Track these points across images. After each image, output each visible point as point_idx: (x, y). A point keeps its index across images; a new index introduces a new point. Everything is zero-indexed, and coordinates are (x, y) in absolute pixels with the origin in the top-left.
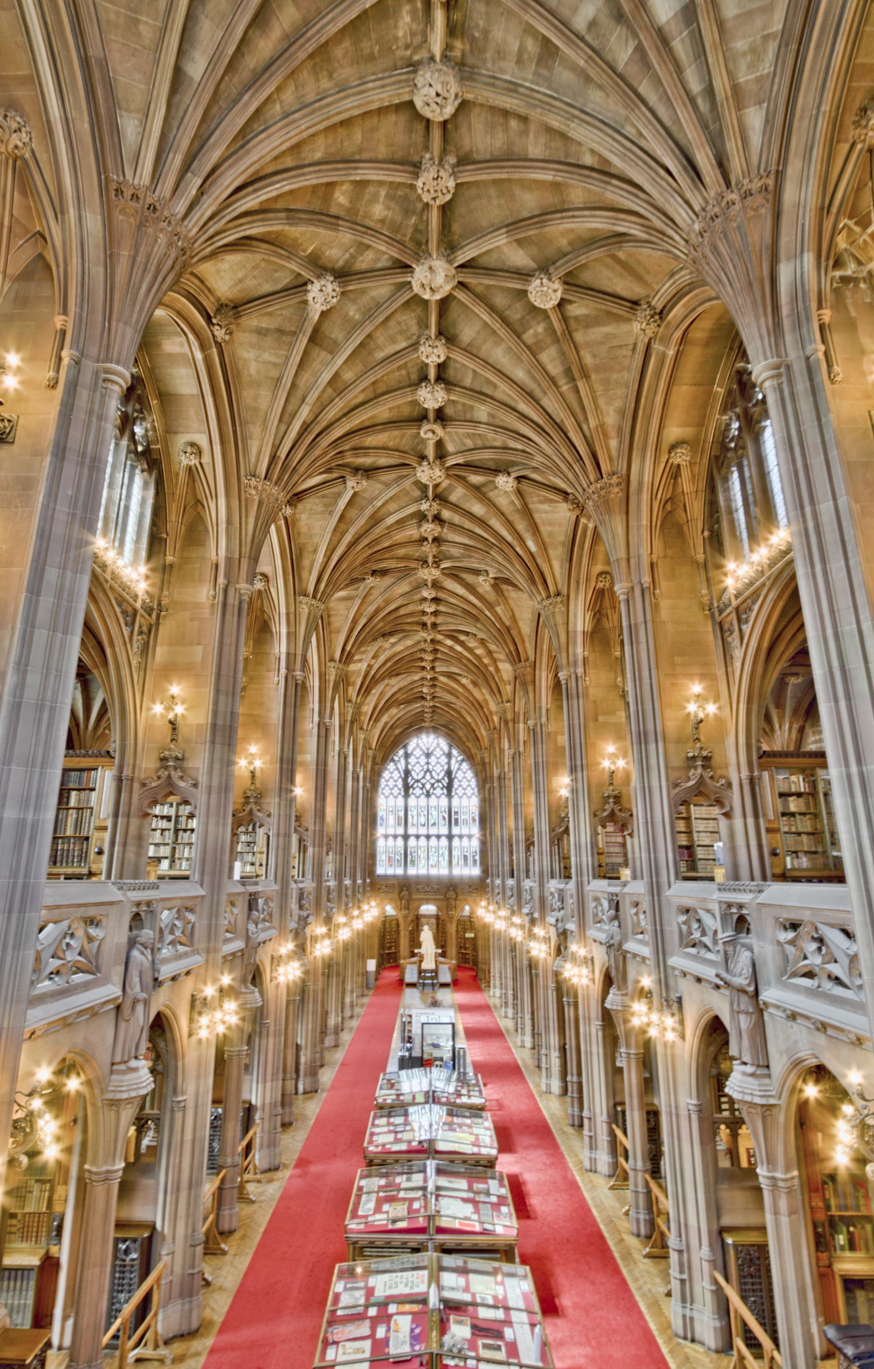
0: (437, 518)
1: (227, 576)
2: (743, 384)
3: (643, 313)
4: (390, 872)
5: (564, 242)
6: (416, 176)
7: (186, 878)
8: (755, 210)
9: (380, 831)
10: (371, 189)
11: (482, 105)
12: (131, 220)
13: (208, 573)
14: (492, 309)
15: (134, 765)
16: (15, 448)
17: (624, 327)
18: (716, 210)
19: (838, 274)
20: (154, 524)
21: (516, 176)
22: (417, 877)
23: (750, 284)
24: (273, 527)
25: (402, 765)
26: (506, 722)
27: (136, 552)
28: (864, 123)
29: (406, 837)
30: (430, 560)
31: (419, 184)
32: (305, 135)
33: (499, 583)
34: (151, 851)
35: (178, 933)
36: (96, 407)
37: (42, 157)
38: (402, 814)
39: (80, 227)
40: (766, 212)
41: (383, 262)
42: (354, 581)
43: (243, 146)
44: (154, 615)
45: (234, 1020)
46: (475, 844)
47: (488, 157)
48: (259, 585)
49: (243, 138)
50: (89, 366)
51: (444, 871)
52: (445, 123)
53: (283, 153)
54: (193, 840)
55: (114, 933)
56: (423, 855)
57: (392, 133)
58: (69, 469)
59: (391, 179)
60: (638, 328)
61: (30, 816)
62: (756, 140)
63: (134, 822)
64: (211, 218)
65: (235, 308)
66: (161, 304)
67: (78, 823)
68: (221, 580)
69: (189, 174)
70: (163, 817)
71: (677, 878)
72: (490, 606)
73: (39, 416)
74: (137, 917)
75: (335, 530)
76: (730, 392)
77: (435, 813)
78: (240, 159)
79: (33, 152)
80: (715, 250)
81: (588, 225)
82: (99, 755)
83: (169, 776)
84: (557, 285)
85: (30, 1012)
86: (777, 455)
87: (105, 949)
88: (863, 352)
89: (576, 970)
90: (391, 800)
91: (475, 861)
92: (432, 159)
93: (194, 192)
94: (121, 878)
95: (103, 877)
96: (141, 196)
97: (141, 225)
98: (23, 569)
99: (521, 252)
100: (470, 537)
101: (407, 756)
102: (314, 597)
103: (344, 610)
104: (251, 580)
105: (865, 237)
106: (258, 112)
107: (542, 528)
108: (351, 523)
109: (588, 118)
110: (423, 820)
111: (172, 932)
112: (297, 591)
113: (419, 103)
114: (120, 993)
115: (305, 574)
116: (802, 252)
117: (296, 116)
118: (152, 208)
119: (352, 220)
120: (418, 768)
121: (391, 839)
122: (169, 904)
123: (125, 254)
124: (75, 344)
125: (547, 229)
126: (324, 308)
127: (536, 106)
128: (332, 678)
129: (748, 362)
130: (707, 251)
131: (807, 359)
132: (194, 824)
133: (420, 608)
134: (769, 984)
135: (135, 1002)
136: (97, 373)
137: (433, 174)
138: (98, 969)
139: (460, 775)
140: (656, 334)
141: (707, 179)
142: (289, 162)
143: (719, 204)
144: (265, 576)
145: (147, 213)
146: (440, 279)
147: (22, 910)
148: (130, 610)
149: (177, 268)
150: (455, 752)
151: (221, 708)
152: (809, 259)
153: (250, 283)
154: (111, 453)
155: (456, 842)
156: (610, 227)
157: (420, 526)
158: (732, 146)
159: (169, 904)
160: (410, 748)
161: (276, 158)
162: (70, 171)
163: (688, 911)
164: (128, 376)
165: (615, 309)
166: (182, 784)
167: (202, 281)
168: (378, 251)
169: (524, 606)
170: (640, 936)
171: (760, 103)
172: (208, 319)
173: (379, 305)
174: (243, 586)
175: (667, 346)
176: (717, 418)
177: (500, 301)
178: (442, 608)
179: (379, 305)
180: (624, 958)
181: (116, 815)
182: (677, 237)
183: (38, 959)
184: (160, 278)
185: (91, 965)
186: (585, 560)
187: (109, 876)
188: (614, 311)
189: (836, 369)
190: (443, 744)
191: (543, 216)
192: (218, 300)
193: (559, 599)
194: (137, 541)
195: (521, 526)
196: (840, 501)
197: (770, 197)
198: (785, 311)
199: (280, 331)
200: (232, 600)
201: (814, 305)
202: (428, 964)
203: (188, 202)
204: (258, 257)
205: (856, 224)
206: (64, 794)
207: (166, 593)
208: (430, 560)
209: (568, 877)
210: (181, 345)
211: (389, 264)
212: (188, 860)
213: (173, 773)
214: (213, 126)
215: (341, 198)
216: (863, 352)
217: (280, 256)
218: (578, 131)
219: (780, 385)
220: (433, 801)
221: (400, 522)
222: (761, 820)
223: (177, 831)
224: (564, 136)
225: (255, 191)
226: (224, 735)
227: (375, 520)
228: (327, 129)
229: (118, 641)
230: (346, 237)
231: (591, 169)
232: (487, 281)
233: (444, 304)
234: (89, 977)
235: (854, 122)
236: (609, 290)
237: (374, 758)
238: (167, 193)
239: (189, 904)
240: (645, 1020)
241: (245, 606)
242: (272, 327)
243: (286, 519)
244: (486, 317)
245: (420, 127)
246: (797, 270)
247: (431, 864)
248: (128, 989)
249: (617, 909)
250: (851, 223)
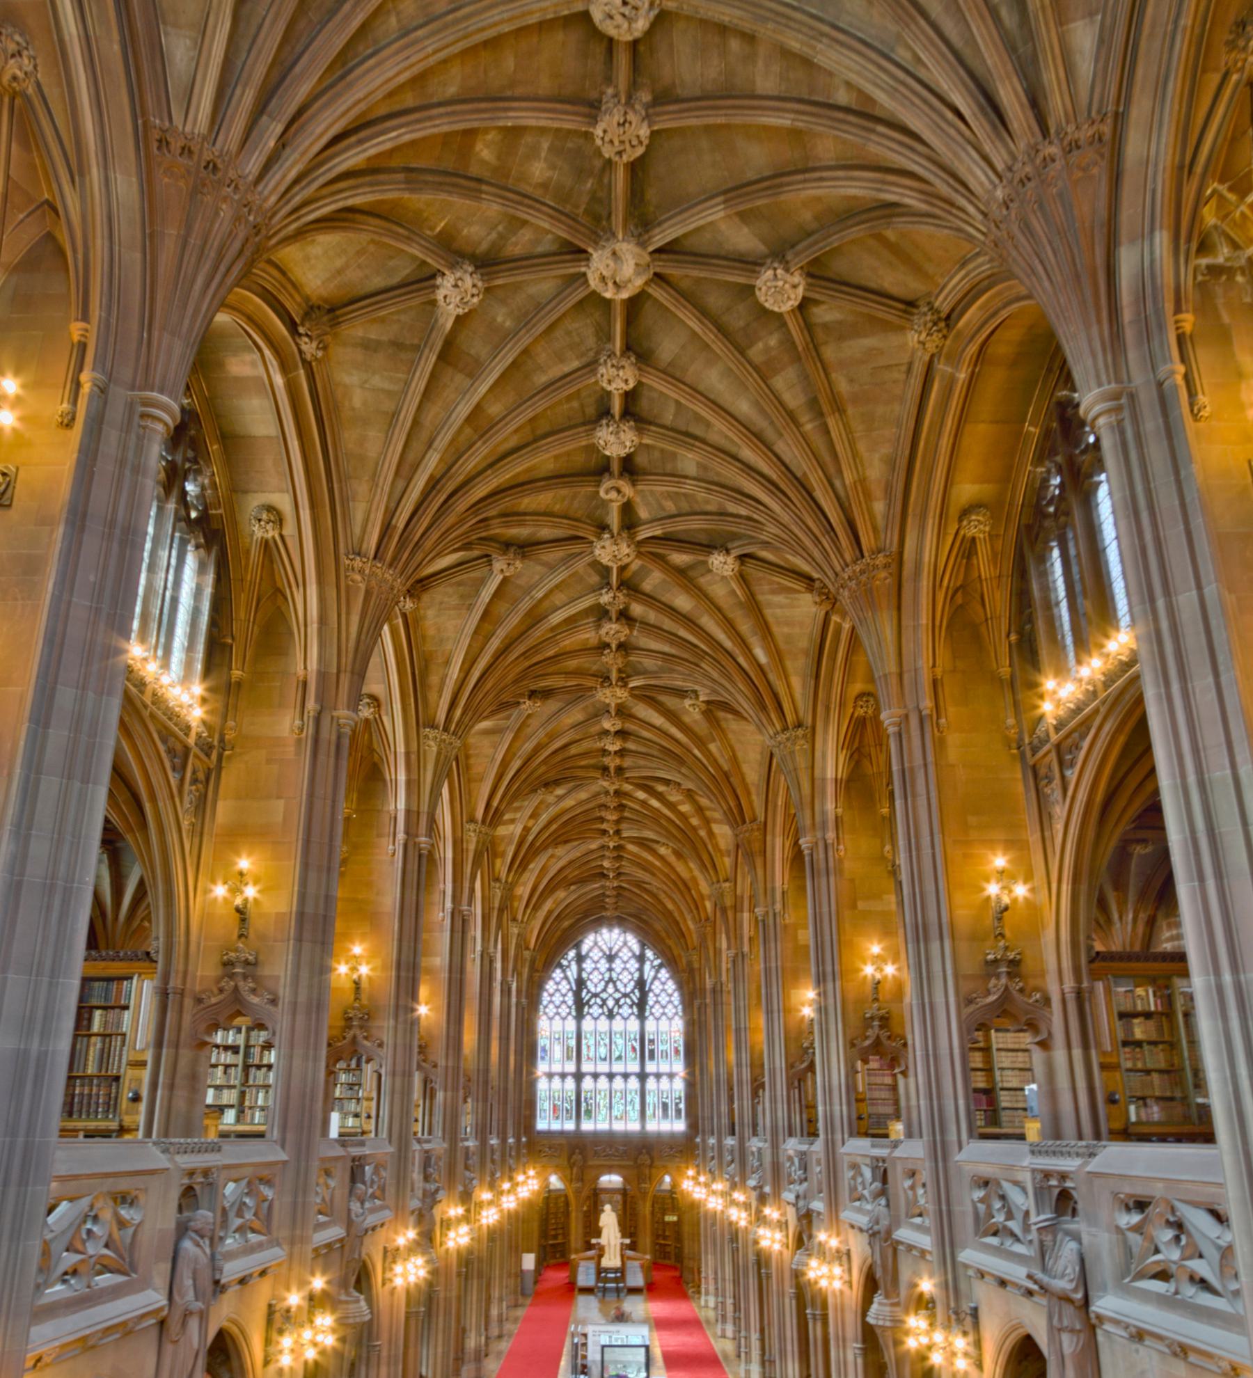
0: (624, 616)
1: (320, 698)
2: (1067, 422)
3: (922, 318)
4: (556, 1126)
5: (807, 216)
6: (594, 120)
7: (260, 1135)
8: (1084, 170)
9: (542, 1067)
10: (528, 139)
11: (689, 18)
12: (181, 184)
13: (293, 695)
14: (704, 313)
15: (185, 973)
16: (13, 514)
17: (894, 340)
18: (1028, 169)
19: (1204, 261)
20: (213, 623)
21: (738, 120)
22: (595, 1134)
23: (1077, 277)
24: (386, 628)
25: (572, 972)
26: (724, 910)
27: (188, 665)
28: (1241, 43)
29: (579, 1076)
30: (614, 676)
31: (599, 132)
32: (432, 61)
33: (713, 709)
34: (209, 1100)
35: (249, 1215)
36: (130, 455)
37: (52, 93)
38: (573, 1043)
39: (105, 195)
40: (1100, 172)
41: (546, 245)
42: (504, 706)
43: (342, 77)
44: (214, 756)
45: (329, 1341)
46: (679, 1085)
47: (698, 93)
48: (366, 712)
49: (343, 65)
50: (120, 395)
51: (634, 1126)
52: (635, 43)
53: (401, 87)
54: (271, 1081)
55: (155, 1215)
56: (603, 1102)
57: (558, 57)
58: (92, 544)
59: (556, 125)
60: (915, 340)
61: (35, 1046)
62: (1085, 67)
63: (186, 1055)
64: (296, 181)
65: (330, 312)
66: (224, 305)
67: (104, 1056)
68: (311, 705)
69: (265, 118)
70: (226, 1048)
71: (971, 1136)
72: (701, 742)
73: (51, 465)
74: (189, 1192)
75: (475, 632)
76: (1047, 434)
77: (620, 1042)
78: (338, 95)
79: (38, 85)
80: (1027, 228)
81: (843, 192)
82: (134, 958)
83: (236, 989)
84: (797, 278)
85: (34, 1330)
86: (1116, 524)
87: (145, 1237)
88: (1240, 375)
89: (825, 1269)
90: (557, 1022)
91: (678, 1111)
92: (616, 95)
93: (272, 143)
94: (166, 1135)
95: (140, 1134)
96: (196, 150)
97: (195, 191)
98: (24, 688)
99: (746, 230)
100: (672, 643)
101: (580, 959)
102: (446, 729)
103: (489, 748)
104: (354, 706)
105: (1243, 208)
106: (364, 28)
107: (776, 630)
108: (499, 622)
109: (841, 37)
110: (603, 1051)
111: (240, 1214)
112: (420, 720)
113: (597, 15)
114: (165, 1302)
115: (432, 696)
116: (1152, 230)
117: (420, 33)
118: (212, 167)
119: (501, 183)
120: (596, 977)
121: (557, 1080)
122: (235, 1174)
123: (171, 234)
124: (99, 363)
125: (783, 197)
126: (460, 311)
127: (768, 19)
128: (472, 847)
129: (1074, 390)
130: (1015, 229)
131: (1160, 384)
132: (271, 1057)
133: (600, 745)
134: (1104, 1288)
135: (187, 1314)
136: (131, 406)
137: (617, 117)
138: (133, 1267)
139: (657, 987)
140: (940, 348)
141: (1015, 125)
142: (409, 100)
143: (1032, 161)
144: (374, 699)
145: (203, 173)
146: (628, 269)
147: (23, 1182)
148: (179, 747)
149: (248, 253)
150: (649, 954)
151: (312, 888)
152: (1162, 240)
153: (353, 275)
154: (151, 522)
155: (651, 1084)
156: (873, 194)
157: (599, 627)
158: (1051, 77)
159: (235, 1174)
160: (585, 948)
161: (390, 95)
162: (91, 112)
163: (986, 1183)
164: (176, 408)
165: (881, 313)
166: (255, 1000)
167: (283, 273)
168: (538, 229)
169: (750, 742)
170: (918, 1220)
171: (1091, 14)
172: (293, 327)
173: (539, 307)
174: (343, 713)
175: (957, 367)
176: (1029, 470)
177: (715, 301)
178: (631, 746)
179: (539, 307)
180: (895, 1251)
181: (159, 1044)
182: (971, 209)
183: (46, 1252)
184: (222, 269)
185: (124, 1262)
186: (838, 675)
187: (148, 1133)
188: (880, 315)
189: (1202, 399)
190: (633, 942)
191: (777, 178)
192: (307, 299)
193: (800, 732)
194: (190, 648)
195: (745, 627)
196: (1206, 591)
197: (1106, 150)
198: (1127, 315)
199: (397, 345)
200: (327, 733)
201: (1169, 306)
202: (611, 1260)
203: (263, 159)
204: (364, 238)
205: (1231, 189)
206: (83, 1014)
207: (231, 723)
208: (614, 676)
209: (814, 1134)
210: (253, 364)
211: (554, 248)
212: (262, 1109)
213: (241, 984)
214: (299, 48)
215: (485, 151)
216: (1240, 375)
217: (397, 236)
218: (829, 56)
219: (1120, 422)
220: (618, 1024)
221: (571, 621)
222: (1093, 1053)
223: (247, 1067)
224: (807, 63)
225: (360, 142)
226: (316, 929)
227: (535, 617)
228: (464, 53)
229: (161, 794)
230: (492, 208)
231: (847, 110)
232: (695, 273)
233: (634, 305)
234: (120, 1279)
235: (1228, 43)
236: (873, 285)
237: (533, 962)
238: (234, 147)
239: (265, 1173)
240: (924, 1340)
241: (346, 742)
242: (384, 338)
243: (404, 616)
244: (694, 324)
245: (599, 50)
246: (1147, 255)
247: (615, 1117)
248: (176, 1297)
249: (884, 1180)
250: (1223, 189)
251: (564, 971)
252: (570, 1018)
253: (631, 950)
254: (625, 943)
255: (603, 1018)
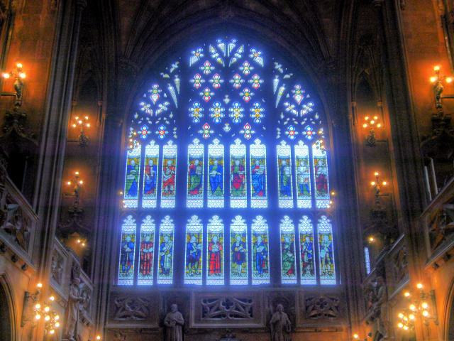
150: (278, 66)
155: (286, 226)
160: (193, 60)
220: (237, 149)
251: (164, 88)
252: (170, 142)
253: (252, 63)
254: (246, 56)
255: (216, 141)
